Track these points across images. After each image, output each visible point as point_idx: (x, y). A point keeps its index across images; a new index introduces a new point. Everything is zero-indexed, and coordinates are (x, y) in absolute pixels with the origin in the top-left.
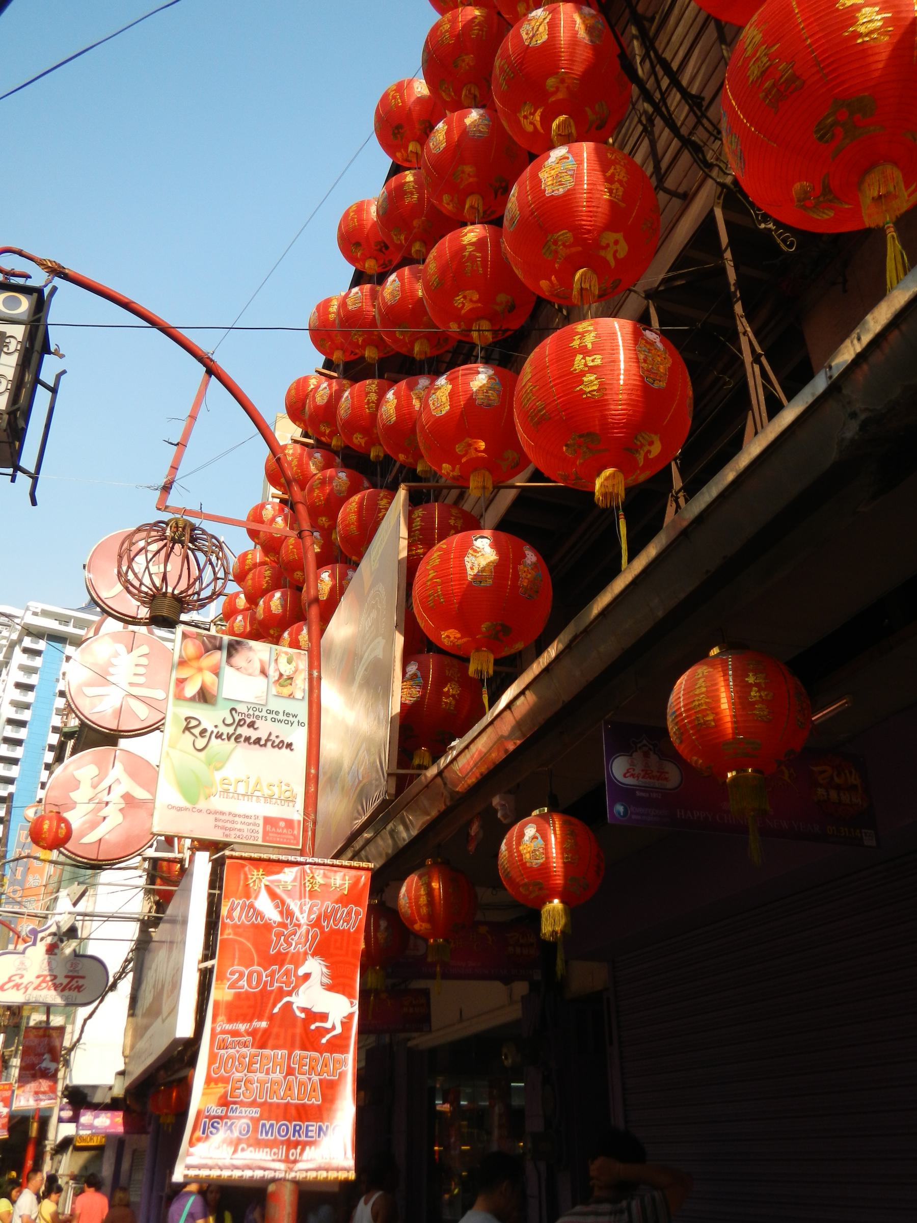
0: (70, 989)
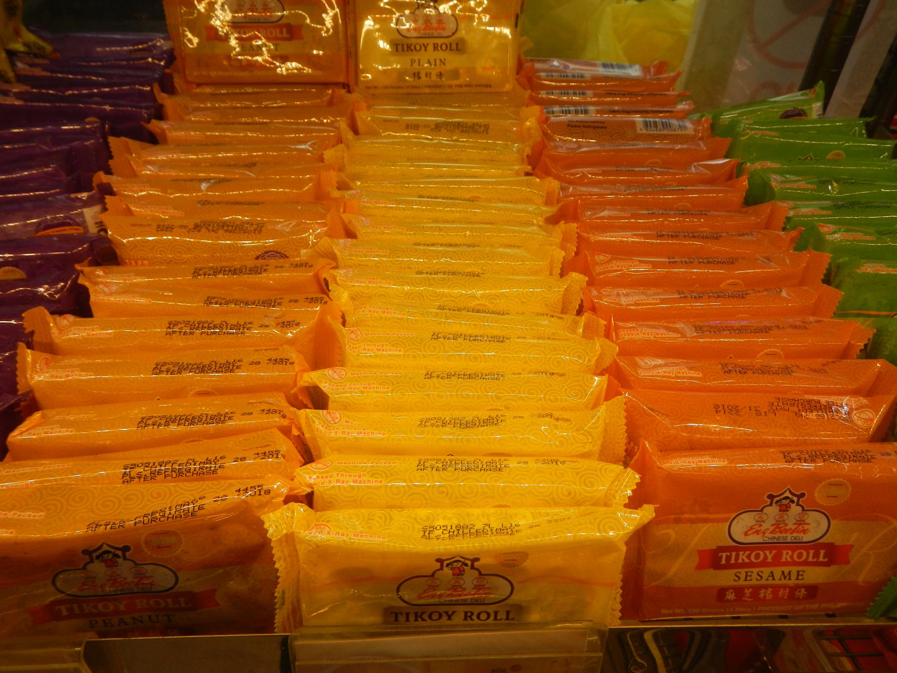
0: (798, 532)
